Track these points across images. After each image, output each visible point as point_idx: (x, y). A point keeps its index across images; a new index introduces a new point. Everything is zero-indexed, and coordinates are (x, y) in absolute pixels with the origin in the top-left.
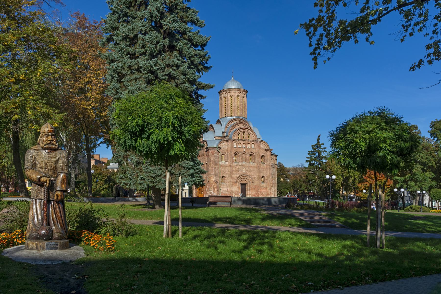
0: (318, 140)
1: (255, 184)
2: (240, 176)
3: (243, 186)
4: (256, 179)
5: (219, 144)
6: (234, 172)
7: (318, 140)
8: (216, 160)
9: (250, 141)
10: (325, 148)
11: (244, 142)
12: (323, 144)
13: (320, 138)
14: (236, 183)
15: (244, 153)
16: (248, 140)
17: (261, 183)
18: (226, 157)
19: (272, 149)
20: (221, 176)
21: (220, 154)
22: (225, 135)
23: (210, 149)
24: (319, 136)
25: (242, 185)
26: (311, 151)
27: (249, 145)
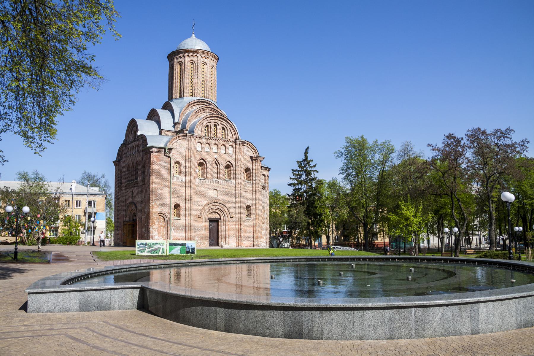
0: (306, 153)
1: (234, 219)
2: (208, 204)
3: (214, 224)
6: (197, 197)
7: (306, 153)
10: (314, 166)
11: (216, 142)
12: (312, 161)
13: (309, 151)
16: (222, 140)
20: (173, 205)
23: (152, 152)
24: (307, 149)
25: (211, 221)
26: (295, 171)
27: (223, 147)
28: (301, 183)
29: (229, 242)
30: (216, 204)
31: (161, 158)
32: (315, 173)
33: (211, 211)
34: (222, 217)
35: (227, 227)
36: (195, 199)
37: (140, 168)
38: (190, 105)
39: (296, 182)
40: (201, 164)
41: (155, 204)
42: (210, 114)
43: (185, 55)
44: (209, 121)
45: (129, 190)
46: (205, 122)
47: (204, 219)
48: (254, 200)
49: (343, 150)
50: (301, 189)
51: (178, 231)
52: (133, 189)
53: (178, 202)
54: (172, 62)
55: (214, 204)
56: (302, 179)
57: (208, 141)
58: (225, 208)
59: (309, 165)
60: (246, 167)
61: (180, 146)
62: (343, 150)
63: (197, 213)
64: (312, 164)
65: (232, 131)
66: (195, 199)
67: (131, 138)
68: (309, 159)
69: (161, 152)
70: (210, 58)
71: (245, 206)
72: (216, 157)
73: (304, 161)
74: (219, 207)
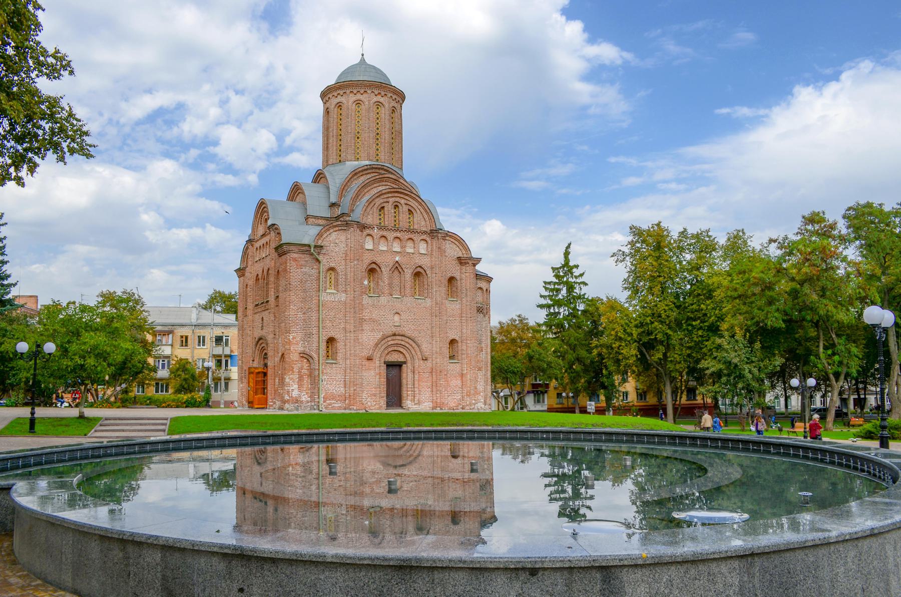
0: (567, 254)
1: (429, 364)
2: (384, 338)
3: (394, 371)
4: (432, 346)
5: (320, 235)
6: (366, 327)
7: (567, 254)
8: (308, 285)
9: (413, 231)
10: (581, 275)
11: (398, 234)
12: (577, 266)
14: (369, 359)
15: (397, 267)
16: (409, 231)
17: (447, 359)
18: (341, 279)
19: (479, 260)
20: (326, 338)
21: (323, 267)
22: (338, 211)
24: (569, 246)
25: (390, 365)
26: (550, 283)
27: (410, 244)
28: (559, 303)
29: (419, 401)
30: (398, 337)
31: (303, 263)
32: (582, 286)
33: (390, 349)
34: (409, 359)
35: (416, 377)
36: (362, 330)
37: (272, 279)
38: (356, 174)
39: (550, 302)
40: (371, 271)
41: (294, 338)
42: (384, 188)
43: (348, 92)
44: (385, 200)
45: (257, 316)
46: (378, 202)
47: (378, 362)
48: (464, 331)
49: (627, 250)
50: (559, 313)
51: (332, 382)
52: (264, 313)
53: (332, 334)
54: (328, 104)
55: (394, 338)
56: (560, 297)
57: (385, 233)
58: (414, 345)
59: (572, 273)
60: (449, 275)
61: (338, 243)
62: (627, 250)
63: (366, 353)
64: (576, 272)
65: (426, 216)
66: (362, 330)
67: (261, 230)
68: (571, 264)
69: (303, 252)
70: (389, 95)
71: (448, 340)
72: (397, 259)
73: (563, 266)
74: (403, 343)
